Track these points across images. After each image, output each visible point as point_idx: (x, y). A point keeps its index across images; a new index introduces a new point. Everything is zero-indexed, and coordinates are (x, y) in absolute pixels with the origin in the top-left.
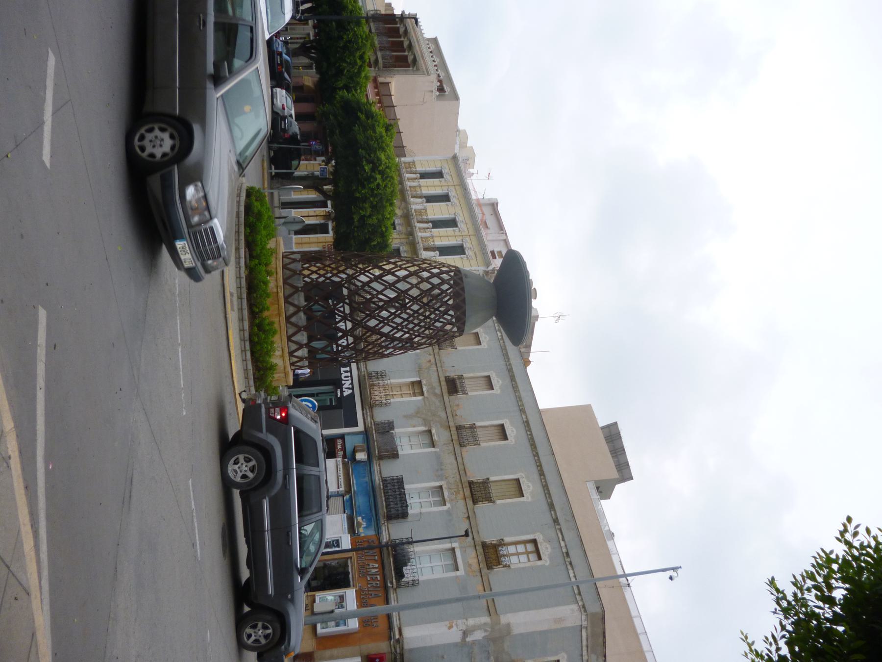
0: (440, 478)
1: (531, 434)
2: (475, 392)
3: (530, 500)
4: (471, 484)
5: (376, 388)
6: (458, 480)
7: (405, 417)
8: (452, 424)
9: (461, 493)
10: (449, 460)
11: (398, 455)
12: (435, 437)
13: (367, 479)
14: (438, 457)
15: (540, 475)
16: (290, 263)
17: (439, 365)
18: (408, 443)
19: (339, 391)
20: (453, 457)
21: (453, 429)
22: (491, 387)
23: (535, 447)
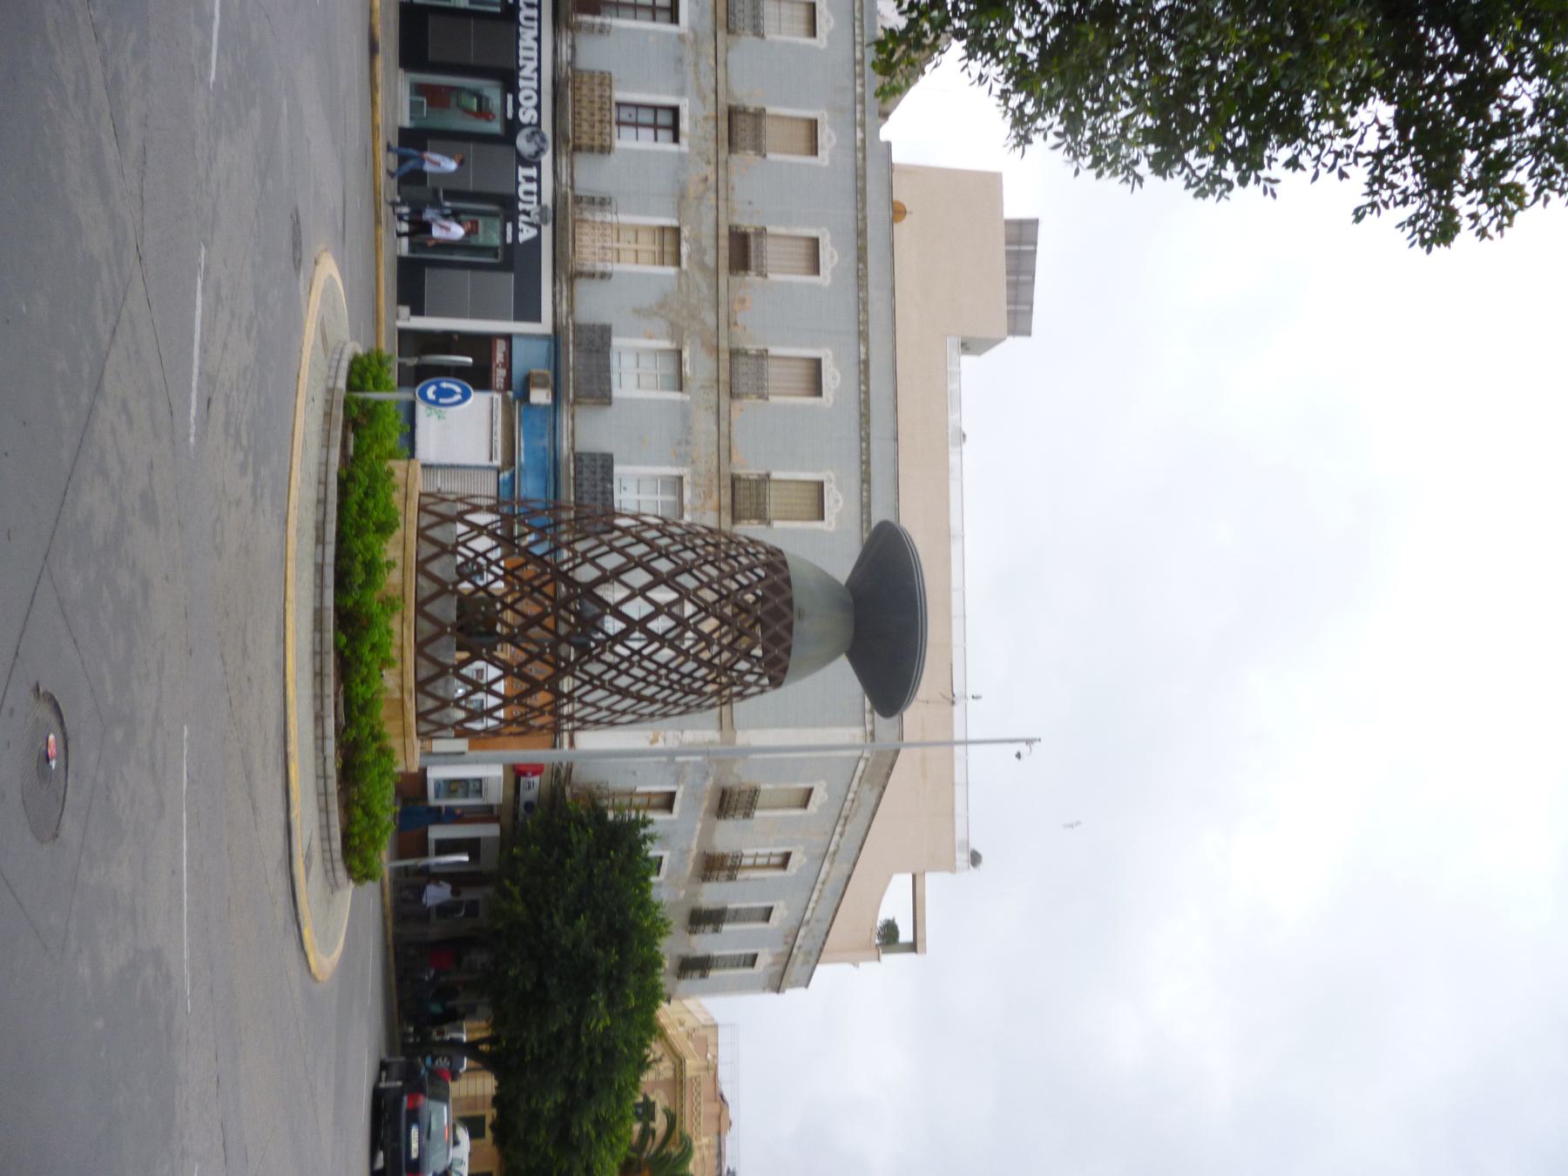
0: (682, 459)
1: (867, 393)
2: (781, 273)
3: (832, 528)
4: (735, 480)
5: (587, 229)
6: (714, 470)
7: (639, 312)
8: (724, 344)
9: (715, 496)
10: (704, 424)
11: (610, 398)
12: (687, 369)
13: (546, 442)
14: (685, 412)
15: (863, 481)
16: (431, 526)
17: (722, 194)
18: (634, 373)
19: (509, 227)
20: (713, 418)
21: (725, 356)
22: (817, 390)
23: (868, 422)
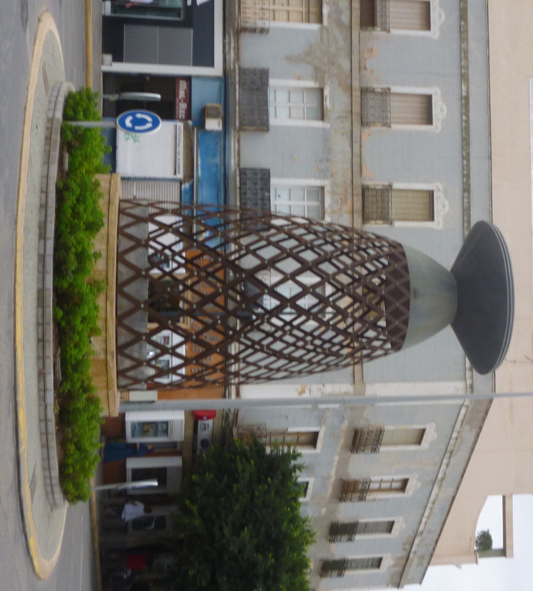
0: (323, 173)
1: (467, 122)
4: (365, 189)
6: (348, 181)
7: (290, 59)
8: (356, 84)
10: (341, 145)
12: (328, 104)
13: (218, 160)
14: (326, 136)
16: (128, 226)
18: (287, 106)
20: (347, 142)
21: (357, 93)
22: (429, 120)
23: (468, 144)
